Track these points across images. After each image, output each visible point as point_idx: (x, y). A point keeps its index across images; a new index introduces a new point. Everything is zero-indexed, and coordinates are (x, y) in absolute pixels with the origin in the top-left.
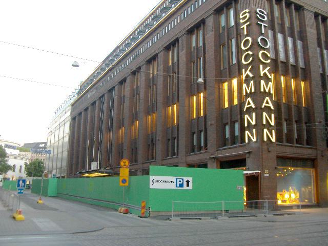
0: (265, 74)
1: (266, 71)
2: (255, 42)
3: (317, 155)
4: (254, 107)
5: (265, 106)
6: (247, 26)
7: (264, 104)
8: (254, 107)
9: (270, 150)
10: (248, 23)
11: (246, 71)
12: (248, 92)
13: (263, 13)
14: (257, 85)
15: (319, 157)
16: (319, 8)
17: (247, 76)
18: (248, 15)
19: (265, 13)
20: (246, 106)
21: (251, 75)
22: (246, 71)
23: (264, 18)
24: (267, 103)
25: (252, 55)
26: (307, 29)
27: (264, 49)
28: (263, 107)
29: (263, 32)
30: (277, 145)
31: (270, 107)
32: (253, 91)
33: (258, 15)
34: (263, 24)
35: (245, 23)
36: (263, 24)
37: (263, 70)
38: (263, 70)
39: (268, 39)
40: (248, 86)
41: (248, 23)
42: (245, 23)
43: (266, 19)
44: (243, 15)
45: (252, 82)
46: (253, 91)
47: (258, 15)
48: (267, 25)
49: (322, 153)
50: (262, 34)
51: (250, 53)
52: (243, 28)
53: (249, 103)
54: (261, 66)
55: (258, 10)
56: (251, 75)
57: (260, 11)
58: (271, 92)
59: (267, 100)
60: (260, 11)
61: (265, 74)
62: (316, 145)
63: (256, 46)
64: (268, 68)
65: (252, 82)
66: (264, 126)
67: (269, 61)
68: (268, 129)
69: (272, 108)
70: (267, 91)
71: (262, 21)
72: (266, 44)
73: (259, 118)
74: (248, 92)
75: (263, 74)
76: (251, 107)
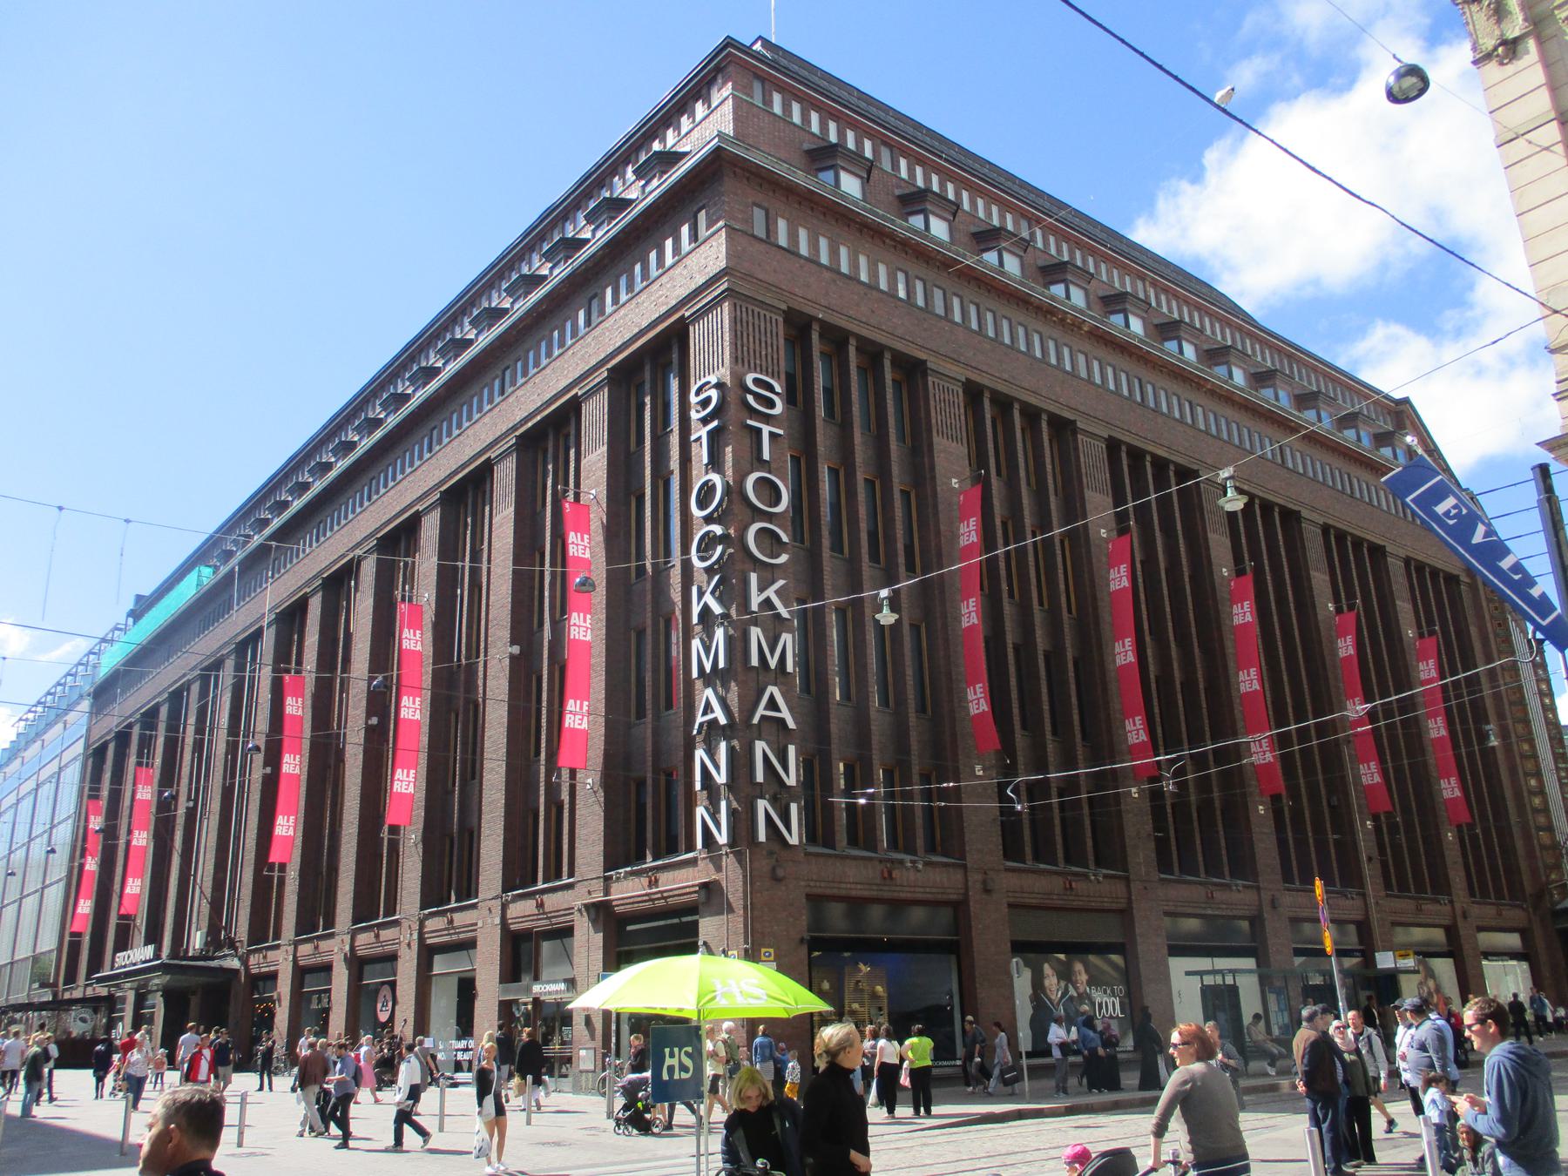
0: (767, 604)
1: (770, 593)
2: (735, 492)
3: (967, 889)
4: (723, 721)
5: (763, 717)
6: (710, 433)
7: (761, 711)
8: (723, 721)
9: (780, 873)
10: (715, 423)
11: (701, 594)
12: (708, 667)
13: (770, 388)
14: (739, 645)
15: (975, 896)
16: (985, 368)
17: (706, 610)
18: (714, 394)
19: (778, 389)
20: (700, 719)
21: (717, 609)
22: (700, 597)
23: (771, 404)
24: (772, 705)
25: (724, 539)
26: (936, 439)
27: (770, 517)
28: (756, 720)
29: (766, 456)
30: (807, 854)
31: (782, 721)
32: (721, 664)
33: (750, 398)
34: (766, 430)
35: (705, 421)
36: (766, 430)
37: (761, 589)
38: (761, 589)
39: (784, 480)
40: (707, 649)
41: (715, 423)
42: (705, 421)
43: (779, 408)
44: (697, 394)
45: (719, 634)
46: (721, 664)
47: (750, 398)
48: (781, 432)
49: (984, 882)
50: (760, 463)
51: (718, 530)
52: (699, 439)
53: (708, 708)
54: (754, 577)
55: (749, 379)
56: (717, 609)
57: (757, 381)
58: (790, 668)
59: (772, 697)
60: (757, 381)
61: (767, 604)
62: (963, 857)
63: (738, 508)
64: (781, 582)
65: (719, 634)
66: (760, 791)
67: (783, 558)
68: (774, 801)
69: (791, 724)
70: (773, 663)
71: (767, 419)
72: (777, 500)
73: (740, 764)
74: (708, 667)
75: (760, 605)
76: (715, 720)
